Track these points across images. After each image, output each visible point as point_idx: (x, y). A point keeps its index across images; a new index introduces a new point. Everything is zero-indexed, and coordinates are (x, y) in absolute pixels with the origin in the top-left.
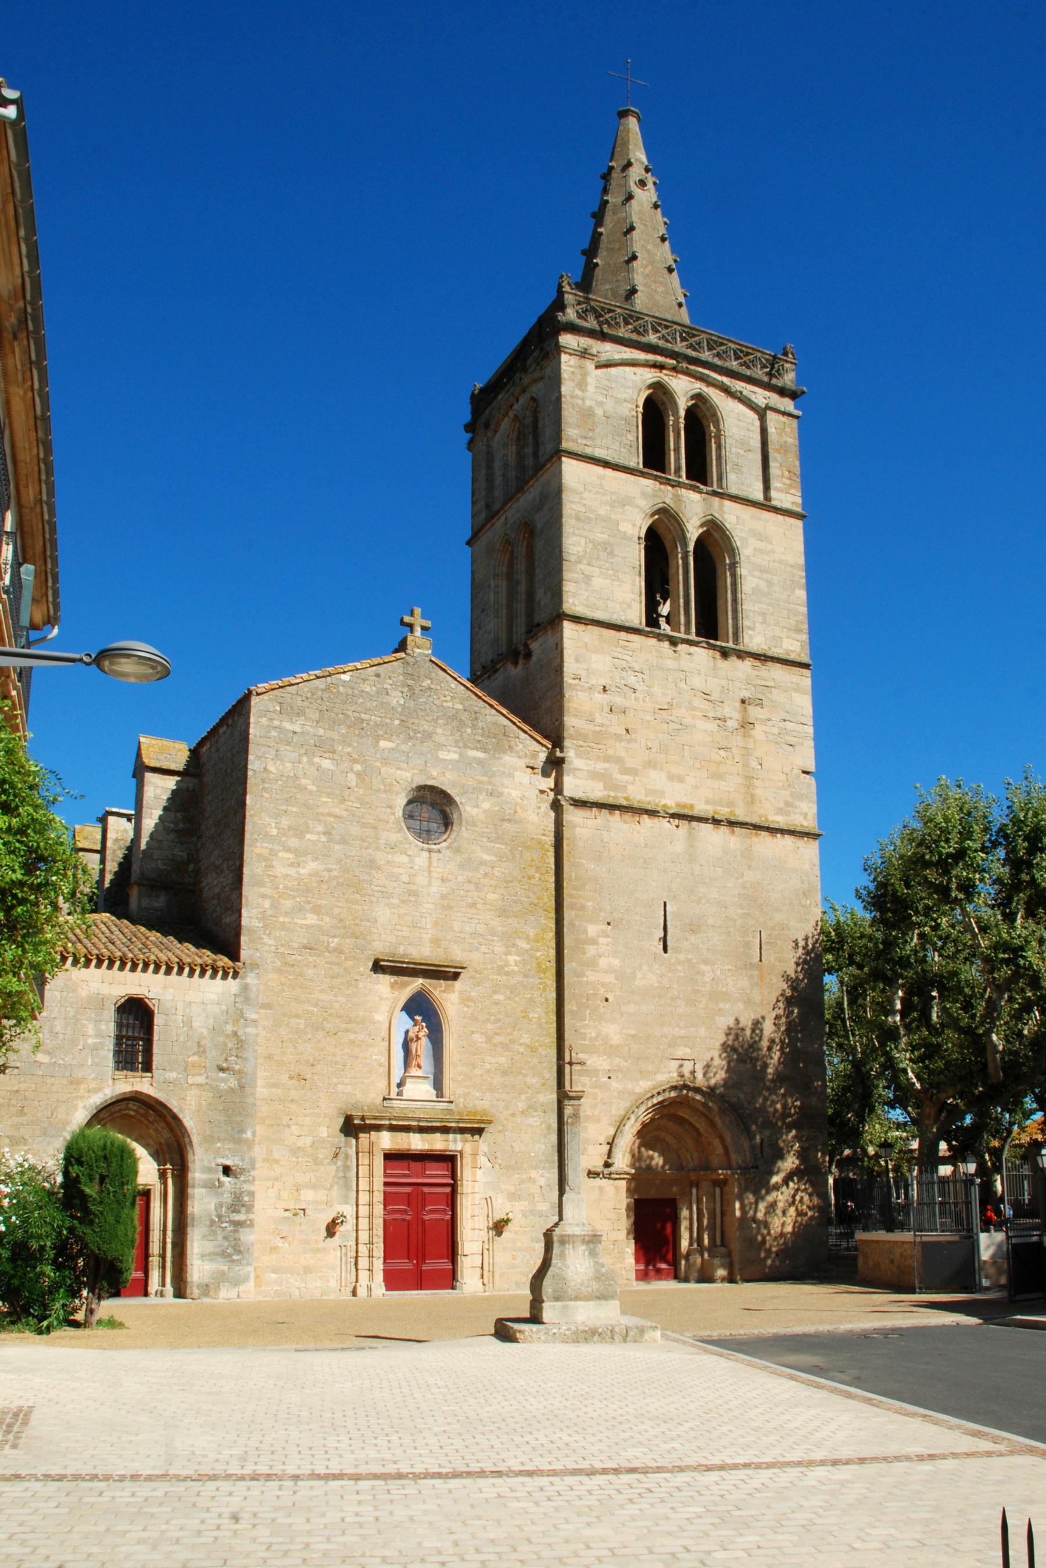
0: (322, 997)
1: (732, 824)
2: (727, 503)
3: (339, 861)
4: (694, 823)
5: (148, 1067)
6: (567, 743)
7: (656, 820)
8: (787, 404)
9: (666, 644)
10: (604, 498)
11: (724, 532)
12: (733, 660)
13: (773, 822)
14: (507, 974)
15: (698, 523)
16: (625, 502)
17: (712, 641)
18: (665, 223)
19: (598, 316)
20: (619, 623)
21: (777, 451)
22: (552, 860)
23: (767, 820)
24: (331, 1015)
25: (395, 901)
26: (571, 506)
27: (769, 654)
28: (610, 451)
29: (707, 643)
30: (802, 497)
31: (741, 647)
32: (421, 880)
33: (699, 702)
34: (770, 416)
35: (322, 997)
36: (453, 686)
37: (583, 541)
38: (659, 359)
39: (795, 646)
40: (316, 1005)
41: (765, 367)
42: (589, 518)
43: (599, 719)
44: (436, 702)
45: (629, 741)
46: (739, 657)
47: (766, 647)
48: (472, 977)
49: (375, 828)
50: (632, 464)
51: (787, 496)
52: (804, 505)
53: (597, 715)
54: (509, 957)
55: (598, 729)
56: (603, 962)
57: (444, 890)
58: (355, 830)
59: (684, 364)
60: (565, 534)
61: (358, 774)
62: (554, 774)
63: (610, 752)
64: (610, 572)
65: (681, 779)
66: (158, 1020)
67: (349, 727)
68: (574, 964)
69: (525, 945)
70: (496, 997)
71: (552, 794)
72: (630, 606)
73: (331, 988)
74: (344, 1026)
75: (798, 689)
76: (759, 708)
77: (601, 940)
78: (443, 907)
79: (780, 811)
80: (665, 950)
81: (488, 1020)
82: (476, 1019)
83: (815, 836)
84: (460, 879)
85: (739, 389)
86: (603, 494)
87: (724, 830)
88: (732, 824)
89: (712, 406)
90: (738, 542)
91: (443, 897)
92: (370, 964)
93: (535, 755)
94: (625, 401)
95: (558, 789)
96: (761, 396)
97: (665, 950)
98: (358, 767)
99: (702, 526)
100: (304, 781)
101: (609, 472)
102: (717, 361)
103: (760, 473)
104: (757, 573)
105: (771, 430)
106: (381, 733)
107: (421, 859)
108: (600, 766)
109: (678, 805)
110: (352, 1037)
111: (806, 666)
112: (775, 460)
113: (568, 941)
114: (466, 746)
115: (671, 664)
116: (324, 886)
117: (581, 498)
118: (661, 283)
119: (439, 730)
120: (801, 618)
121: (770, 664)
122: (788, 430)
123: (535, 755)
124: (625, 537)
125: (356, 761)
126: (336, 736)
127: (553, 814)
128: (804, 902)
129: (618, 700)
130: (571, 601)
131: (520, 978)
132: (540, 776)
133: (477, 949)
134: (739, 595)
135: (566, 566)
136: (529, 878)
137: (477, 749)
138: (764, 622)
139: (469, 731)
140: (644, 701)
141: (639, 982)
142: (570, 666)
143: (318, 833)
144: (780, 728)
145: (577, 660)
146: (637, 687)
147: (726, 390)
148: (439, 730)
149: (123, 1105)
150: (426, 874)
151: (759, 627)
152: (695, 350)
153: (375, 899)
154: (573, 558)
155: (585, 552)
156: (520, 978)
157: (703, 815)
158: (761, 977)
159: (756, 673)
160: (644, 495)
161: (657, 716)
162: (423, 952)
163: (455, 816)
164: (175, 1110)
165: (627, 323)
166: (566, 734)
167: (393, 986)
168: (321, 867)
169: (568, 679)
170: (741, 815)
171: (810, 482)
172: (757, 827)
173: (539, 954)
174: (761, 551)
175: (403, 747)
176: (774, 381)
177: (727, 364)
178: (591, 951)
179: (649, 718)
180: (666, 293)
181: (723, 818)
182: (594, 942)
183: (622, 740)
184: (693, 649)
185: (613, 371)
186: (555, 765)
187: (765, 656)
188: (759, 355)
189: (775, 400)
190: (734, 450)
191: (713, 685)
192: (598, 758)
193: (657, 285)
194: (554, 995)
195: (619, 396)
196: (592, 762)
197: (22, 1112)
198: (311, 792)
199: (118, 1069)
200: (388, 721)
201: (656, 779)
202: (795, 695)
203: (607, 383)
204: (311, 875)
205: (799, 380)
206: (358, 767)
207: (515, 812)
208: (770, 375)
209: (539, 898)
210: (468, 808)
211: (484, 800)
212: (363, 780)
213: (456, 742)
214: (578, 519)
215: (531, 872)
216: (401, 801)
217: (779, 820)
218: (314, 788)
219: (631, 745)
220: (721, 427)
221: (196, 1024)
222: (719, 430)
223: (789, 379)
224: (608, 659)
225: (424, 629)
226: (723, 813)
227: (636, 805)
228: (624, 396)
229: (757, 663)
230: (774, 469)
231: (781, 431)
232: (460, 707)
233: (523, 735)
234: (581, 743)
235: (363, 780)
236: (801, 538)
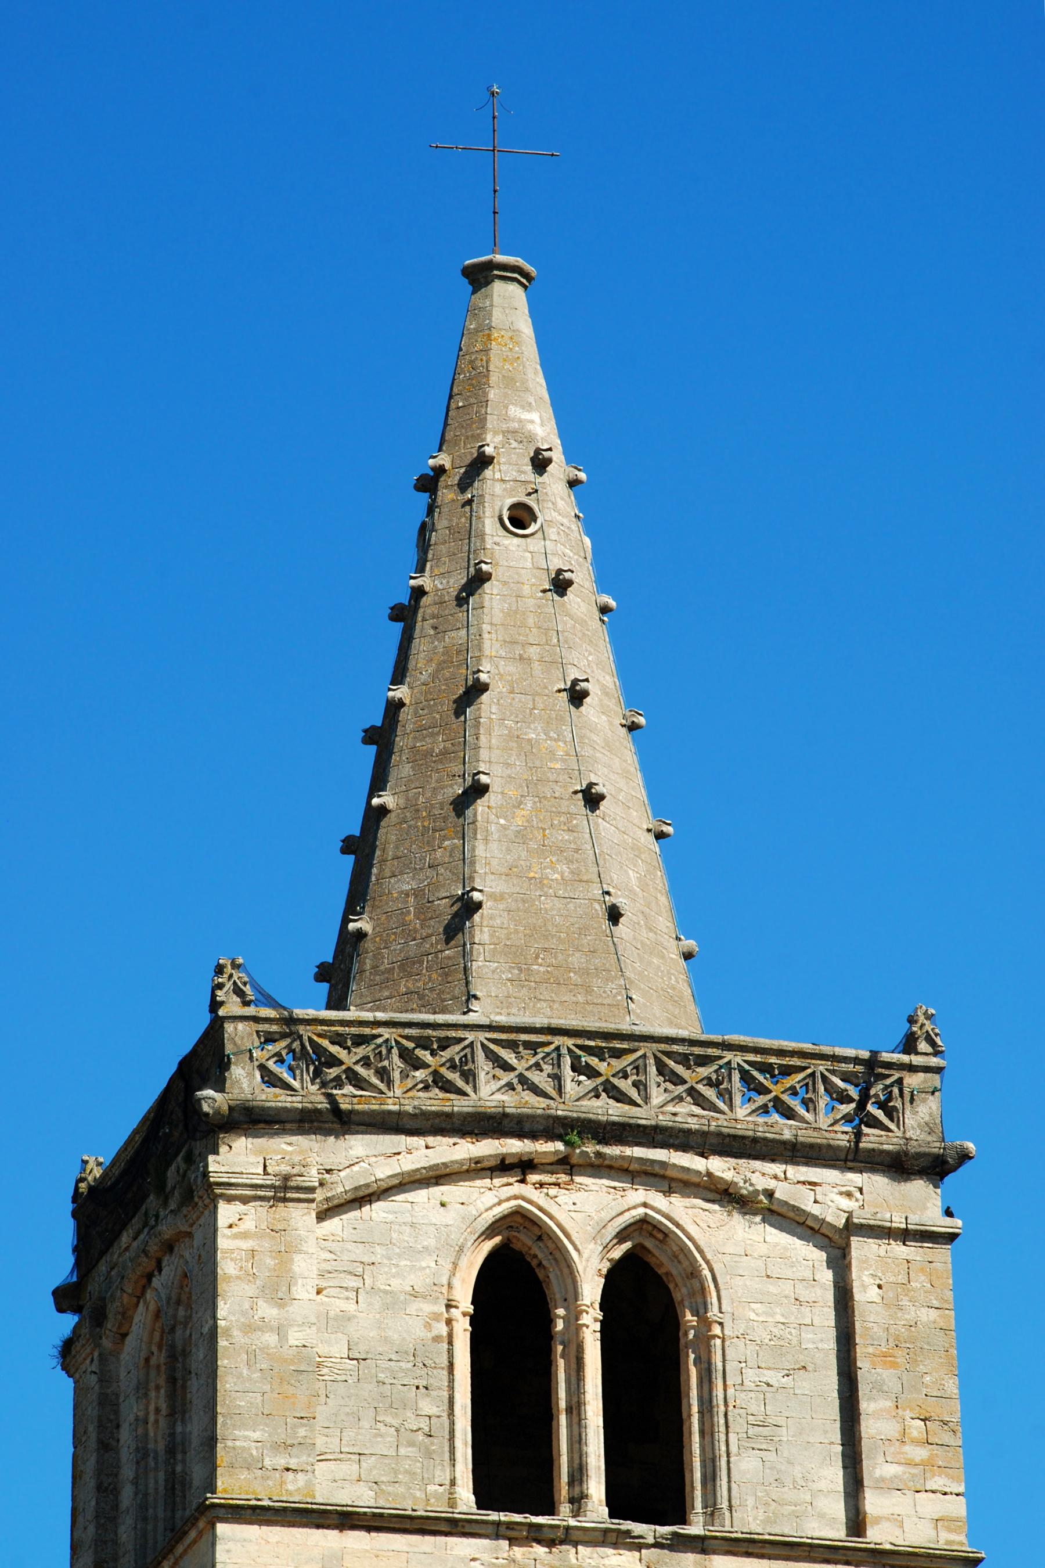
8: (921, 1202)
21: (886, 1359)
28: (367, 1463)
34: (861, 1249)
38: (514, 1146)
59: (583, 1145)
85: (761, 1183)
89: (683, 1249)
96: (833, 1194)
101: (356, 1540)
102: (687, 1115)
103: (837, 1437)
105: (865, 1293)
112: (879, 1388)
147: (725, 1195)
152: (620, 1097)
177: (718, 1122)
185: (378, 1210)
188: (822, 1067)
190: (751, 1376)
195: (395, 1283)
208: (862, 1119)
220: (713, 1313)
222: (706, 1323)
223: (918, 1124)
228: (418, 1281)
230: (874, 1425)
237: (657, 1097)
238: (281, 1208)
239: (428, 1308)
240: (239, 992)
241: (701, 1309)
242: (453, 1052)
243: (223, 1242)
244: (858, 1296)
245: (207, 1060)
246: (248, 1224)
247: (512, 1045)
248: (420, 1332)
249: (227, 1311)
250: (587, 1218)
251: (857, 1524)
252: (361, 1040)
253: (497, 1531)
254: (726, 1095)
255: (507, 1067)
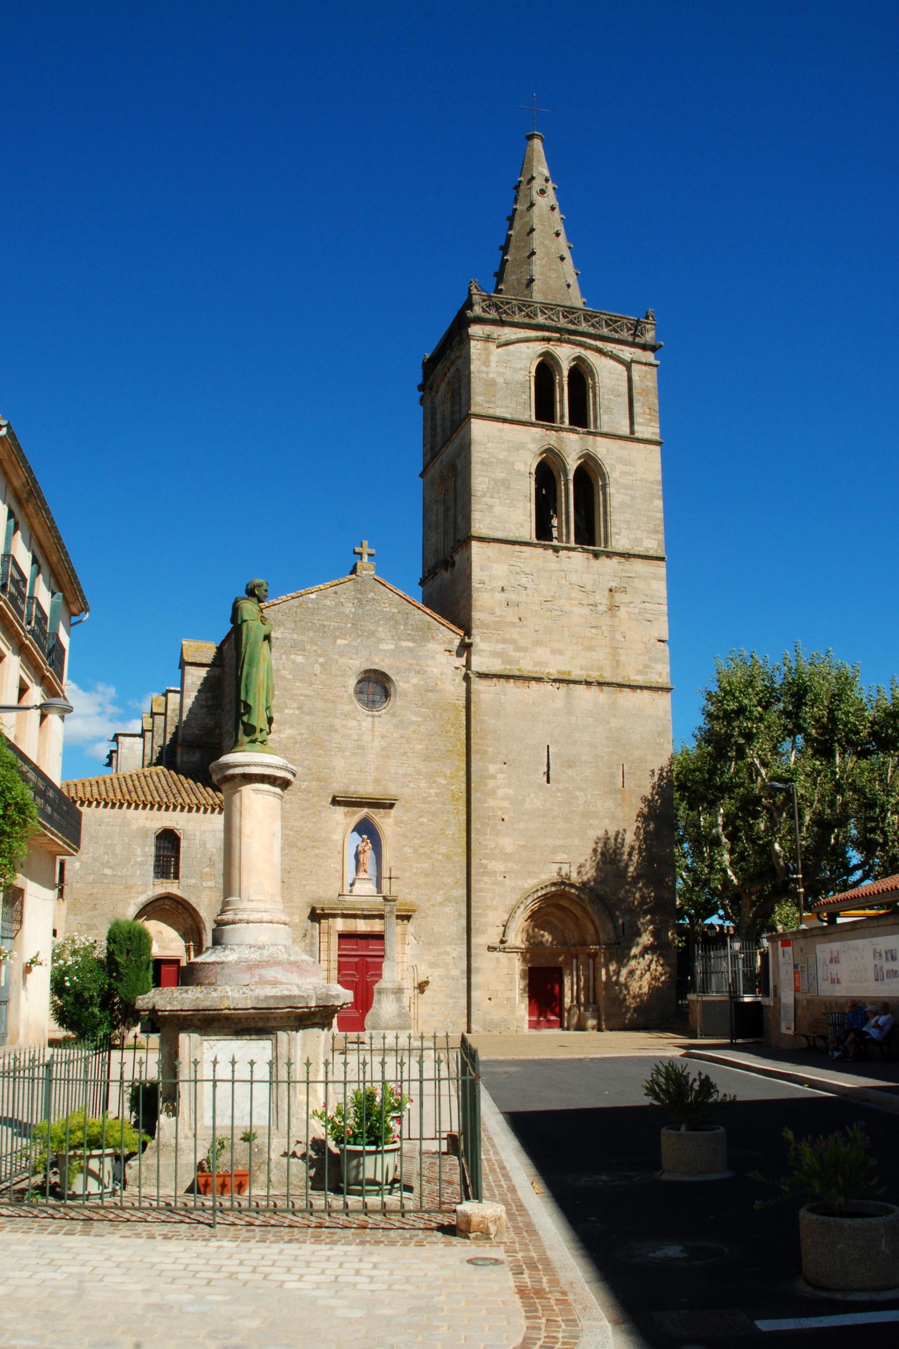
0: (296, 824)
1: (600, 684)
2: (599, 439)
3: (308, 727)
4: (571, 685)
5: (177, 877)
6: (474, 631)
7: (542, 684)
8: (649, 357)
9: (551, 551)
10: (503, 446)
11: (597, 461)
12: (603, 560)
13: (634, 680)
14: (429, 803)
15: (577, 457)
16: (519, 447)
17: (586, 547)
18: (562, 219)
19: (498, 308)
20: (514, 539)
21: (640, 394)
22: (464, 718)
23: (629, 680)
24: (302, 836)
25: (348, 754)
26: (478, 455)
27: (631, 552)
29: (582, 548)
30: (660, 427)
31: (609, 549)
32: (367, 737)
33: (576, 594)
34: (635, 367)
35: (296, 824)
36: (390, 596)
37: (487, 480)
38: (547, 334)
39: (653, 544)
40: (291, 830)
41: (631, 329)
42: (492, 462)
43: (498, 612)
44: (379, 609)
45: (521, 627)
46: (608, 556)
47: (629, 547)
48: (404, 806)
49: (333, 702)
50: (525, 418)
51: (648, 428)
52: (662, 434)
53: (497, 609)
54: (431, 791)
55: (498, 619)
56: (500, 792)
57: (384, 744)
58: (319, 704)
59: (565, 335)
60: (473, 476)
61: (322, 665)
62: (465, 655)
63: (507, 636)
64: (508, 501)
65: (561, 653)
66: (183, 844)
67: (315, 631)
68: (479, 794)
69: (444, 782)
70: (421, 820)
71: (464, 669)
72: (522, 526)
73: (302, 817)
74: (311, 844)
75: (656, 578)
76: (623, 594)
77: (499, 776)
78: (383, 756)
79: (639, 672)
80: (548, 781)
81: (416, 837)
82: (406, 837)
83: (668, 690)
84: (395, 735)
85: (609, 349)
86: (502, 443)
87: (595, 689)
88: (600, 684)
89: (589, 365)
90: (607, 468)
91: (383, 749)
92: (330, 799)
93: (451, 642)
94: (521, 369)
95: (468, 665)
96: (627, 353)
97: (548, 781)
98: (321, 660)
99: (579, 458)
100: (283, 672)
101: (507, 426)
102: (592, 330)
103: (628, 413)
104: (622, 491)
105: (635, 378)
106: (338, 634)
107: (367, 723)
108: (500, 647)
109: (559, 672)
110: (317, 851)
111: (662, 559)
112: (638, 401)
113: (474, 778)
114: (400, 639)
115: (553, 566)
116: (298, 746)
117: (486, 448)
118: (554, 270)
119: (380, 629)
120: (658, 522)
121: (633, 559)
122: (649, 376)
123: (451, 642)
124: (519, 474)
125: (320, 656)
126: (305, 638)
127: (464, 684)
128: (658, 741)
129: (513, 597)
130: (477, 526)
131: (439, 806)
132: (455, 656)
133: (408, 786)
134: (608, 509)
135: (474, 500)
136: (446, 732)
137: (408, 640)
138: (628, 528)
139: (402, 627)
140: (533, 596)
141: (527, 806)
142: (477, 574)
143: (294, 709)
144: (640, 608)
145: (482, 570)
146: (527, 586)
147: (600, 351)
148: (380, 629)
149: (161, 902)
150: (370, 733)
151: (624, 532)
152: (574, 324)
153: (333, 753)
154: (479, 494)
155: (488, 488)
156: (439, 806)
157: (578, 679)
158: (623, 800)
159: (622, 567)
160: (534, 440)
161: (543, 606)
162: (368, 790)
163: (392, 690)
164: (194, 905)
165: (521, 310)
166: (473, 625)
167: (346, 814)
168: (295, 732)
169: (475, 584)
170: (608, 677)
171: (667, 415)
172: (620, 686)
173: (453, 787)
174: (626, 473)
175: (354, 643)
176: (638, 340)
177: (599, 332)
178: (491, 784)
179: (536, 608)
180: (559, 277)
181: (593, 680)
182: (493, 777)
183: (515, 627)
184: (571, 554)
185: (511, 347)
186: (465, 648)
187: (628, 554)
188: (625, 321)
189: (638, 354)
190: (606, 396)
191: (587, 580)
192: (498, 641)
193: (553, 268)
194: (465, 817)
195: (516, 366)
196: (493, 645)
197: (95, 908)
198: (288, 680)
199: (157, 878)
200: (343, 625)
201: (542, 653)
202: (654, 582)
203: (507, 358)
204: (288, 738)
205: (658, 336)
206: (321, 660)
207: (437, 684)
208: (635, 335)
209: (454, 746)
210: (401, 684)
211: (413, 677)
212: (325, 669)
213: (393, 636)
214: (483, 463)
215: (448, 727)
216: (353, 682)
217: (639, 679)
218: (291, 677)
219: (523, 630)
220: (596, 380)
221: (208, 846)
222: (594, 383)
223: (649, 336)
224: (506, 566)
225: (369, 555)
226: (594, 675)
227: (526, 674)
228: (521, 366)
229: (623, 560)
230: (637, 408)
231: (643, 378)
232: (396, 610)
233: (442, 628)
234: (485, 631)
235: (325, 669)
236: (659, 460)
237: (584, 325)
238: (487, 344)
239: (524, 373)
240: (476, 288)
241: (593, 379)
242: (532, 308)
243: (472, 350)
244: (634, 378)
245: (469, 304)
246: (479, 347)
247: (546, 308)
248: (522, 378)
249: (473, 368)
250: (565, 354)
251: (632, 432)
252: (508, 303)
253: (543, 426)
254: (601, 326)
255: (545, 314)
